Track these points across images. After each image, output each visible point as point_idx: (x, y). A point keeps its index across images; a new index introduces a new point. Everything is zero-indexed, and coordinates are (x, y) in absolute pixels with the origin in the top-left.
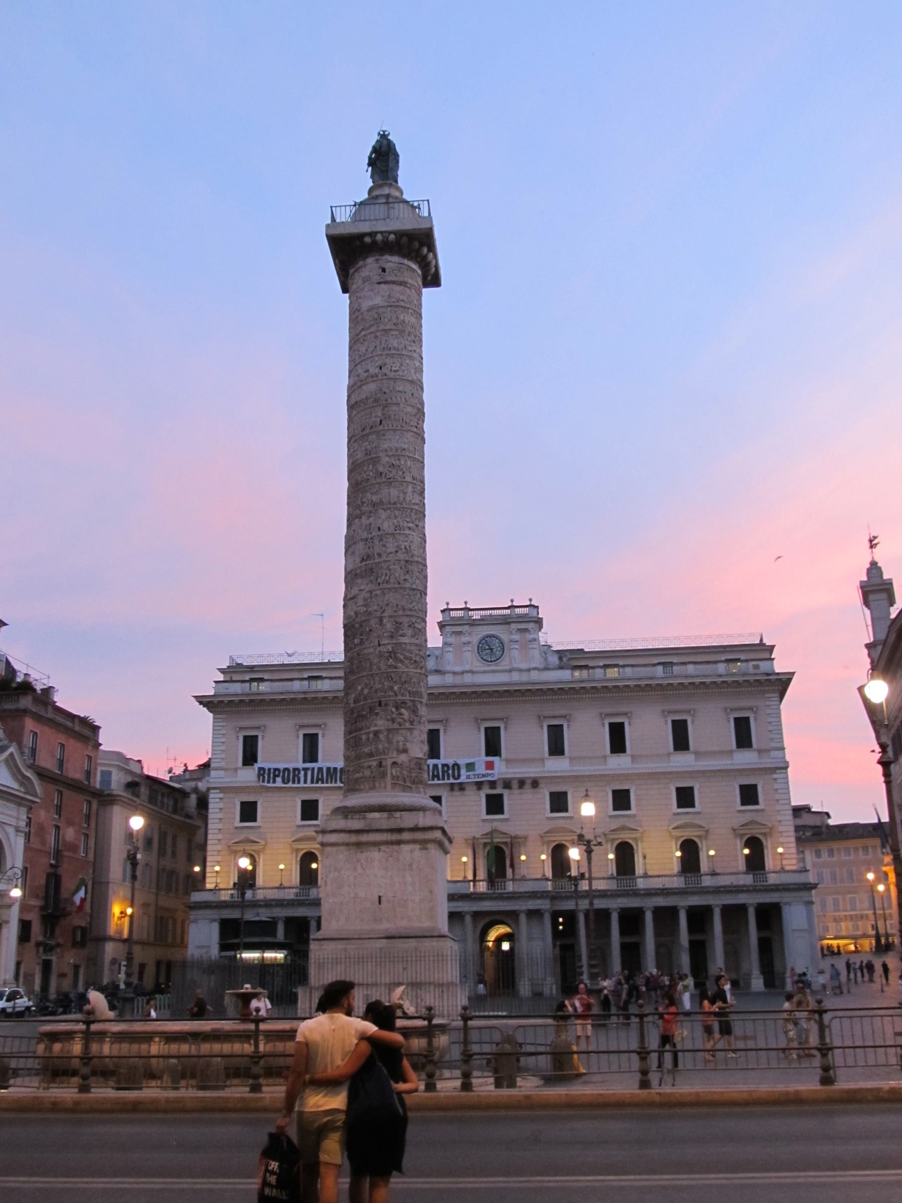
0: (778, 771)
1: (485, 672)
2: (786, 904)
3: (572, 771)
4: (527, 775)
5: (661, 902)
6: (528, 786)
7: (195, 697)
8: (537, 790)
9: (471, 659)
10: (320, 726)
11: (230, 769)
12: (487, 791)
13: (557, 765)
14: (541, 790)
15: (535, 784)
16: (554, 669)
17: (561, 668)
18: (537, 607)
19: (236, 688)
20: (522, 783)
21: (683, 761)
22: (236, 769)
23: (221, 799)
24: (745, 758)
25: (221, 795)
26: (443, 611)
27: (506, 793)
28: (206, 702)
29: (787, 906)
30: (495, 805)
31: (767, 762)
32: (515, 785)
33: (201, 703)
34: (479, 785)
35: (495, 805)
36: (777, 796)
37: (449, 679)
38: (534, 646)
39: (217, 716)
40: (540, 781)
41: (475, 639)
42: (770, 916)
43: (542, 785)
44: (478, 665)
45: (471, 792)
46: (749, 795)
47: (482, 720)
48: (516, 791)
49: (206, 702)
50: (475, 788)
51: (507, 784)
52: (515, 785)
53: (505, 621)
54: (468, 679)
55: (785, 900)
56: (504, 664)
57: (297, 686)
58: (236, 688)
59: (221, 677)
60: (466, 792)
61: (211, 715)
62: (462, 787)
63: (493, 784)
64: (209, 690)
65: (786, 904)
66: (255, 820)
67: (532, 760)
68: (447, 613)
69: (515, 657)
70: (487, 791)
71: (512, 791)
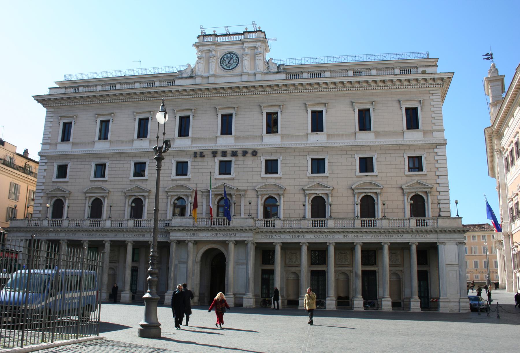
0: (438, 147)
1: (224, 76)
2: (442, 243)
3: (282, 144)
4: (249, 147)
5: (341, 238)
6: (249, 155)
7: (33, 96)
8: (255, 158)
9: (214, 67)
10: (111, 114)
11: (53, 144)
12: (220, 158)
13: (272, 140)
14: (259, 158)
15: (255, 153)
16: (274, 73)
17: (278, 73)
18: (264, 32)
19: (63, 91)
20: (245, 153)
21: (366, 138)
22: (56, 144)
23: (46, 163)
24: (413, 137)
25: (46, 161)
26: (198, 37)
27: (233, 159)
28: (41, 100)
29: (443, 246)
30: (225, 168)
31: (429, 140)
32: (240, 154)
33: (39, 101)
34: (214, 154)
35: (225, 168)
36: (437, 165)
37: (198, 80)
38: (260, 58)
39: (50, 110)
40: (259, 152)
41: (219, 55)
42: (428, 253)
43: (258, 155)
44: (220, 71)
45: (209, 158)
46: (416, 163)
47: (219, 108)
48: (242, 158)
49: (41, 100)
50: (212, 155)
51: (234, 154)
52: (240, 154)
53: (242, 43)
54: (211, 80)
55: (441, 240)
56: (238, 70)
57: (99, 88)
58: (63, 91)
59: (58, 86)
60: (205, 159)
61: (45, 110)
62: (202, 155)
63: (224, 154)
64: (45, 92)
65: (442, 243)
66: (65, 177)
67: (254, 138)
68: (201, 38)
69: (246, 65)
70: (220, 158)
71: (237, 158)
